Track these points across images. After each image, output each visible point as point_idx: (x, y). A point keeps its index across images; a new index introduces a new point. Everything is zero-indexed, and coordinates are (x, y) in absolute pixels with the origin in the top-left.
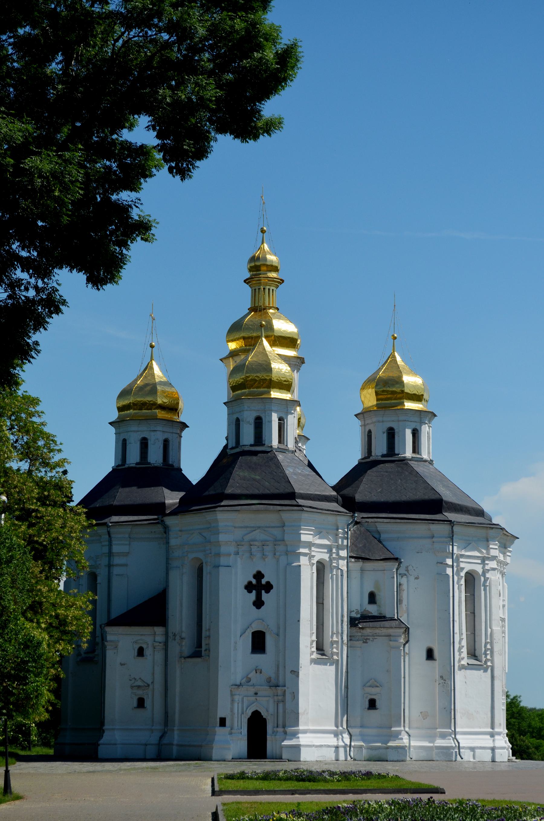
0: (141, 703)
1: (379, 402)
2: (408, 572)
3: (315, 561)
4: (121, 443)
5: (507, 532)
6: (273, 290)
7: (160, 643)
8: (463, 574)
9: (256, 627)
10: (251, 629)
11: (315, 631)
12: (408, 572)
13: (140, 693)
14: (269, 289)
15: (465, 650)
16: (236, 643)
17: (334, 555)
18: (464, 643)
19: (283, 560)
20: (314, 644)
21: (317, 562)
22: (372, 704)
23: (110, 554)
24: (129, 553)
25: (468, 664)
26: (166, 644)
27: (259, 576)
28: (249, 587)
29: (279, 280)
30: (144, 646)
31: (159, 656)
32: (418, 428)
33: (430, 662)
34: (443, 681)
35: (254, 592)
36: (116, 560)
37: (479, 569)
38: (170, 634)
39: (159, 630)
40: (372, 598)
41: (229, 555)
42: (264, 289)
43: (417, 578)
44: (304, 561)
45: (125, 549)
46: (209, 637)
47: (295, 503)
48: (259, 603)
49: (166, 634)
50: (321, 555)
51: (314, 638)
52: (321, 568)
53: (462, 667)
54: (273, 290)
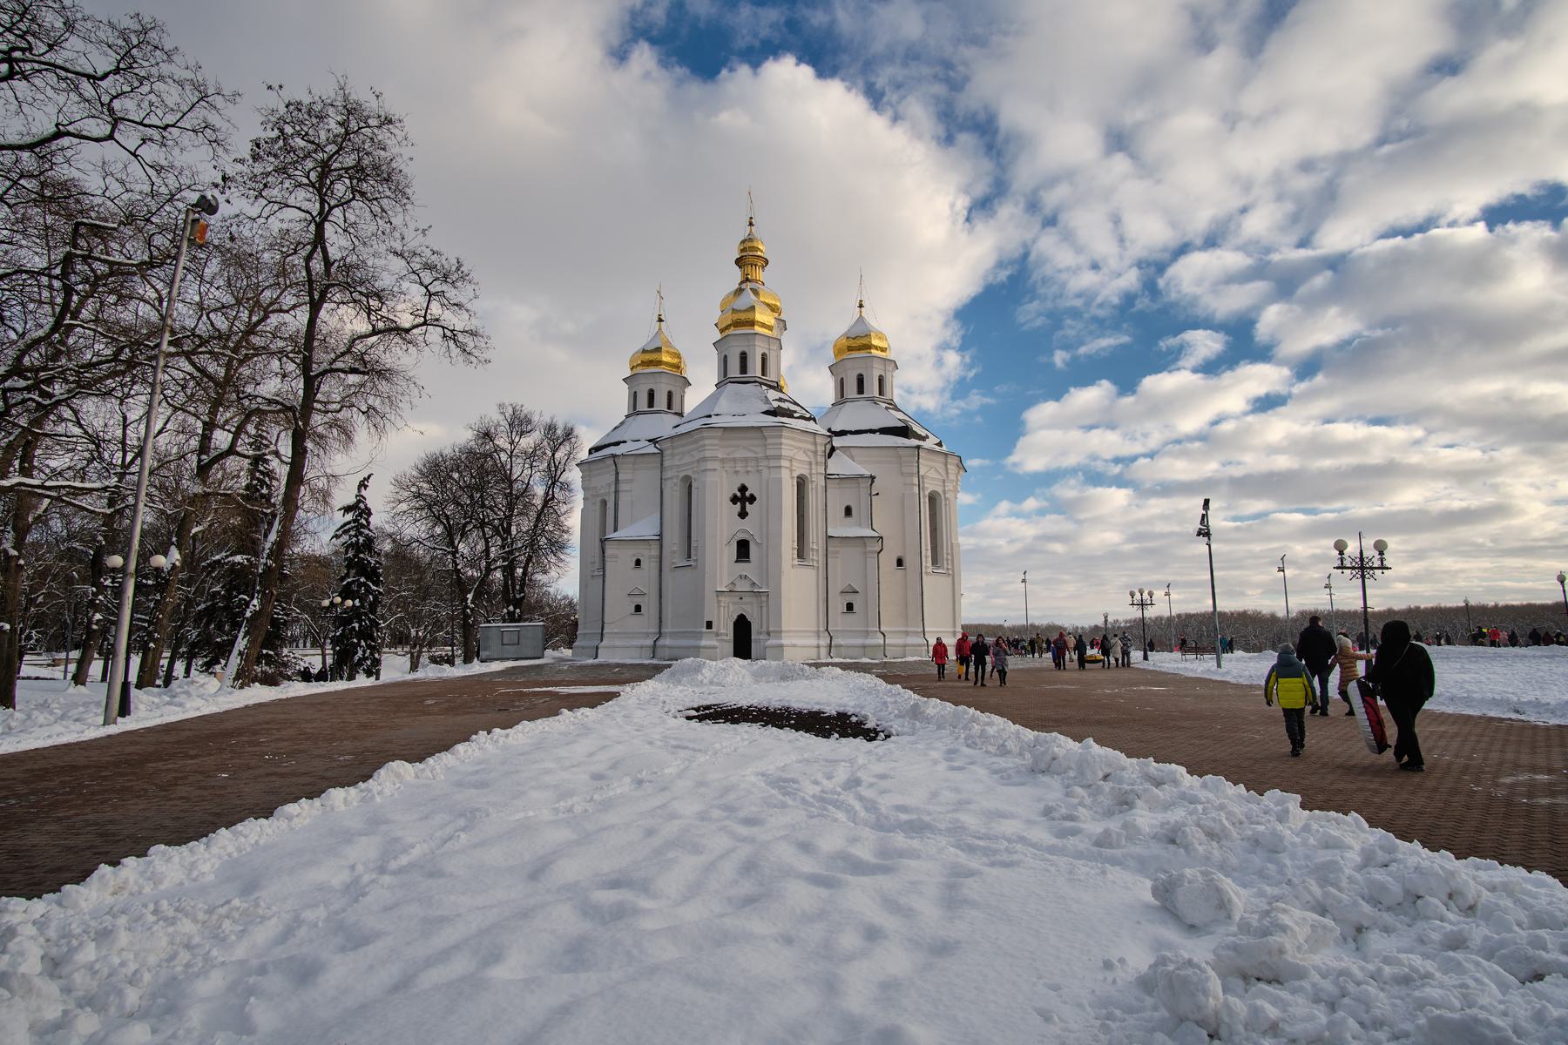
0: (638, 608)
3: (796, 474)
8: (927, 493)
11: (796, 539)
13: (638, 601)
15: (930, 559)
17: (813, 471)
18: (929, 553)
19: (765, 472)
20: (796, 552)
22: (850, 607)
27: (743, 489)
28: (734, 500)
31: (655, 565)
33: (900, 573)
37: (939, 489)
45: (629, 477)
48: (743, 514)
50: (801, 470)
51: (795, 545)
52: (802, 483)
53: (926, 573)
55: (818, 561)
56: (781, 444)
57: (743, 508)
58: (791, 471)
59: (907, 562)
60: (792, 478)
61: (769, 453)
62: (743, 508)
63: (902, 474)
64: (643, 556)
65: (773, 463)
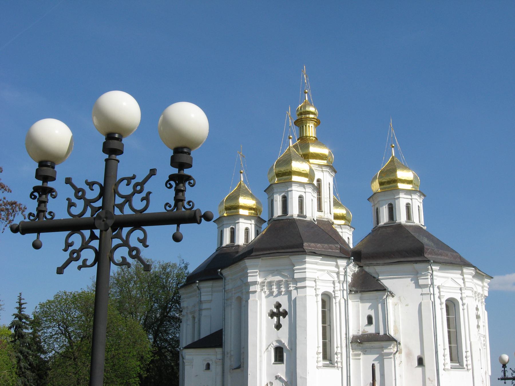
1: (382, 187)
2: (400, 301)
3: (320, 292)
4: (220, 232)
5: (479, 270)
6: (312, 127)
7: (220, 360)
8: (444, 300)
9: (276, 344)
10: (273, 346)
12: (400, 301)
14: (309, 126)
16: (261, 356)
17: (336, 289)
20: (321, 356)
21: (323, 294)
23: (200, 302)
24: (211, 300)
25: (451, 368)
26: (223, 359)
27: (278, 306)
28: (272, 315)
29: (316, 120)
30: (210, 362)
31: (219, 369)
32: (410, 201)
34: (431, 382)
35: (275, 318)
36: (204, 306)
37: (457, 297)
38: (226, 353)
39: (219, 350)
40: (370, 320)
41: (255, 292)
42: (306, 126)
43: (407, 305)
44: (310, 292)
46: (244, 353)
47: (303, 250)
48: (278, 326)
49: (223, 354)
51: (321, 350)
54: (312, 127)
55: (342, 363)
56: (305, 268)
57: (279, 320)
58: (315, 289)
59: (426, 361)
60: (317, 295)
61: (296, 276)
62: (279, 320)
63: (418, 286)
64: (211, 360)
65: (299, 285)
